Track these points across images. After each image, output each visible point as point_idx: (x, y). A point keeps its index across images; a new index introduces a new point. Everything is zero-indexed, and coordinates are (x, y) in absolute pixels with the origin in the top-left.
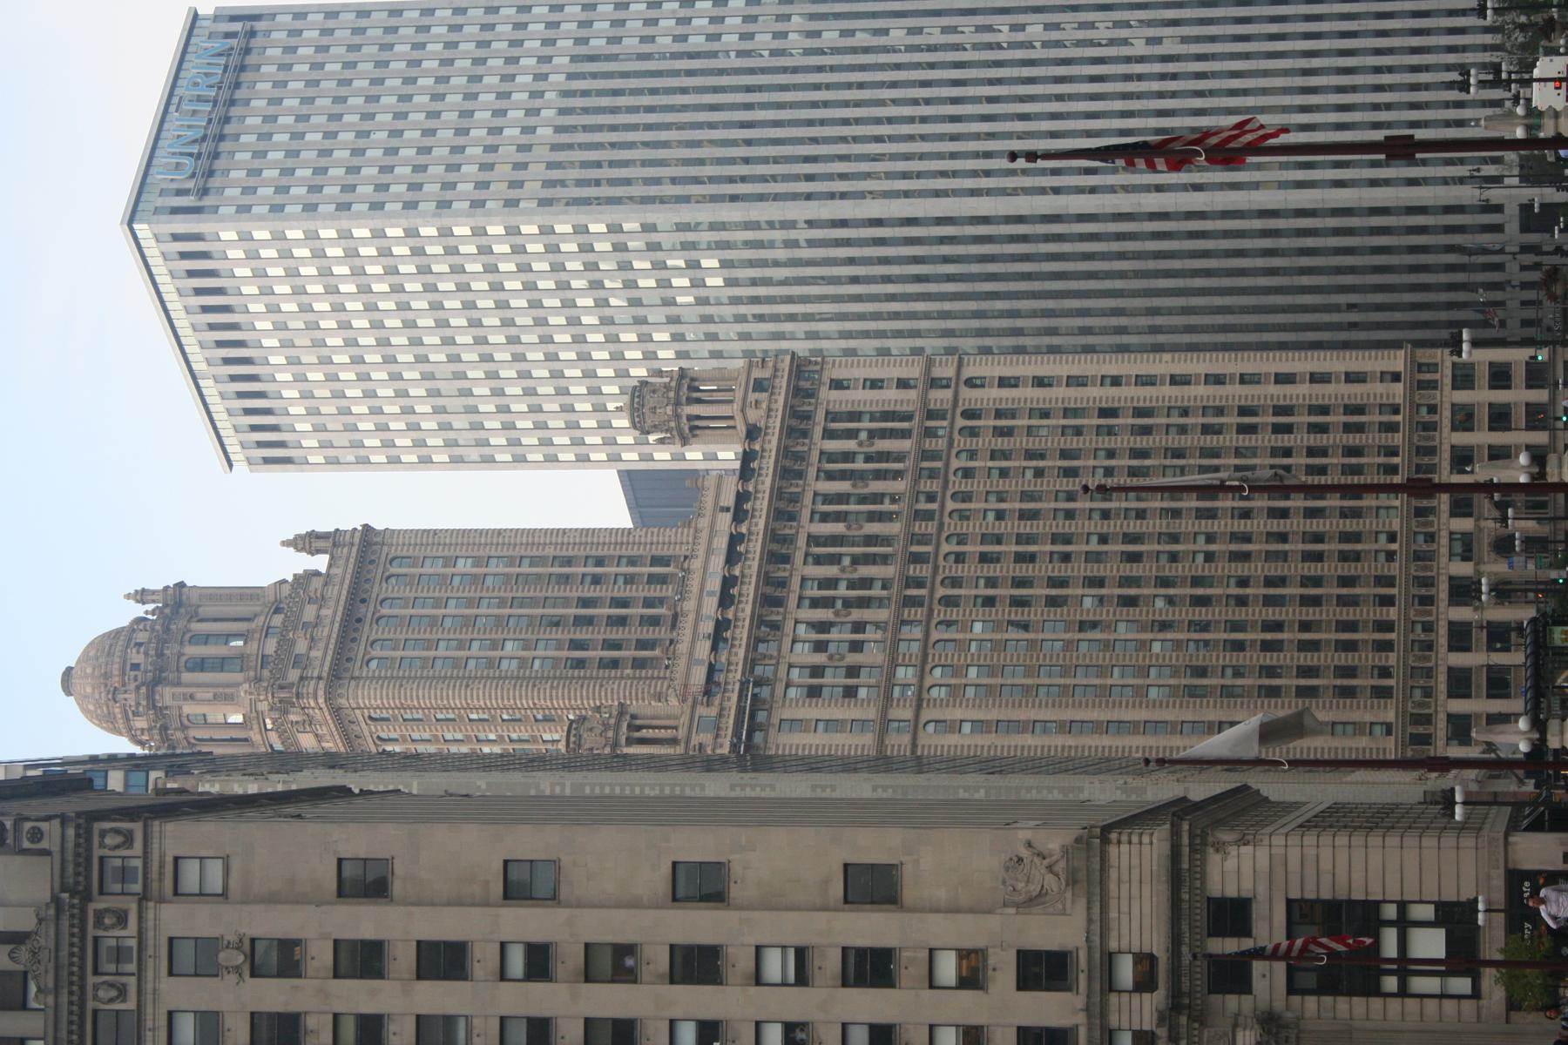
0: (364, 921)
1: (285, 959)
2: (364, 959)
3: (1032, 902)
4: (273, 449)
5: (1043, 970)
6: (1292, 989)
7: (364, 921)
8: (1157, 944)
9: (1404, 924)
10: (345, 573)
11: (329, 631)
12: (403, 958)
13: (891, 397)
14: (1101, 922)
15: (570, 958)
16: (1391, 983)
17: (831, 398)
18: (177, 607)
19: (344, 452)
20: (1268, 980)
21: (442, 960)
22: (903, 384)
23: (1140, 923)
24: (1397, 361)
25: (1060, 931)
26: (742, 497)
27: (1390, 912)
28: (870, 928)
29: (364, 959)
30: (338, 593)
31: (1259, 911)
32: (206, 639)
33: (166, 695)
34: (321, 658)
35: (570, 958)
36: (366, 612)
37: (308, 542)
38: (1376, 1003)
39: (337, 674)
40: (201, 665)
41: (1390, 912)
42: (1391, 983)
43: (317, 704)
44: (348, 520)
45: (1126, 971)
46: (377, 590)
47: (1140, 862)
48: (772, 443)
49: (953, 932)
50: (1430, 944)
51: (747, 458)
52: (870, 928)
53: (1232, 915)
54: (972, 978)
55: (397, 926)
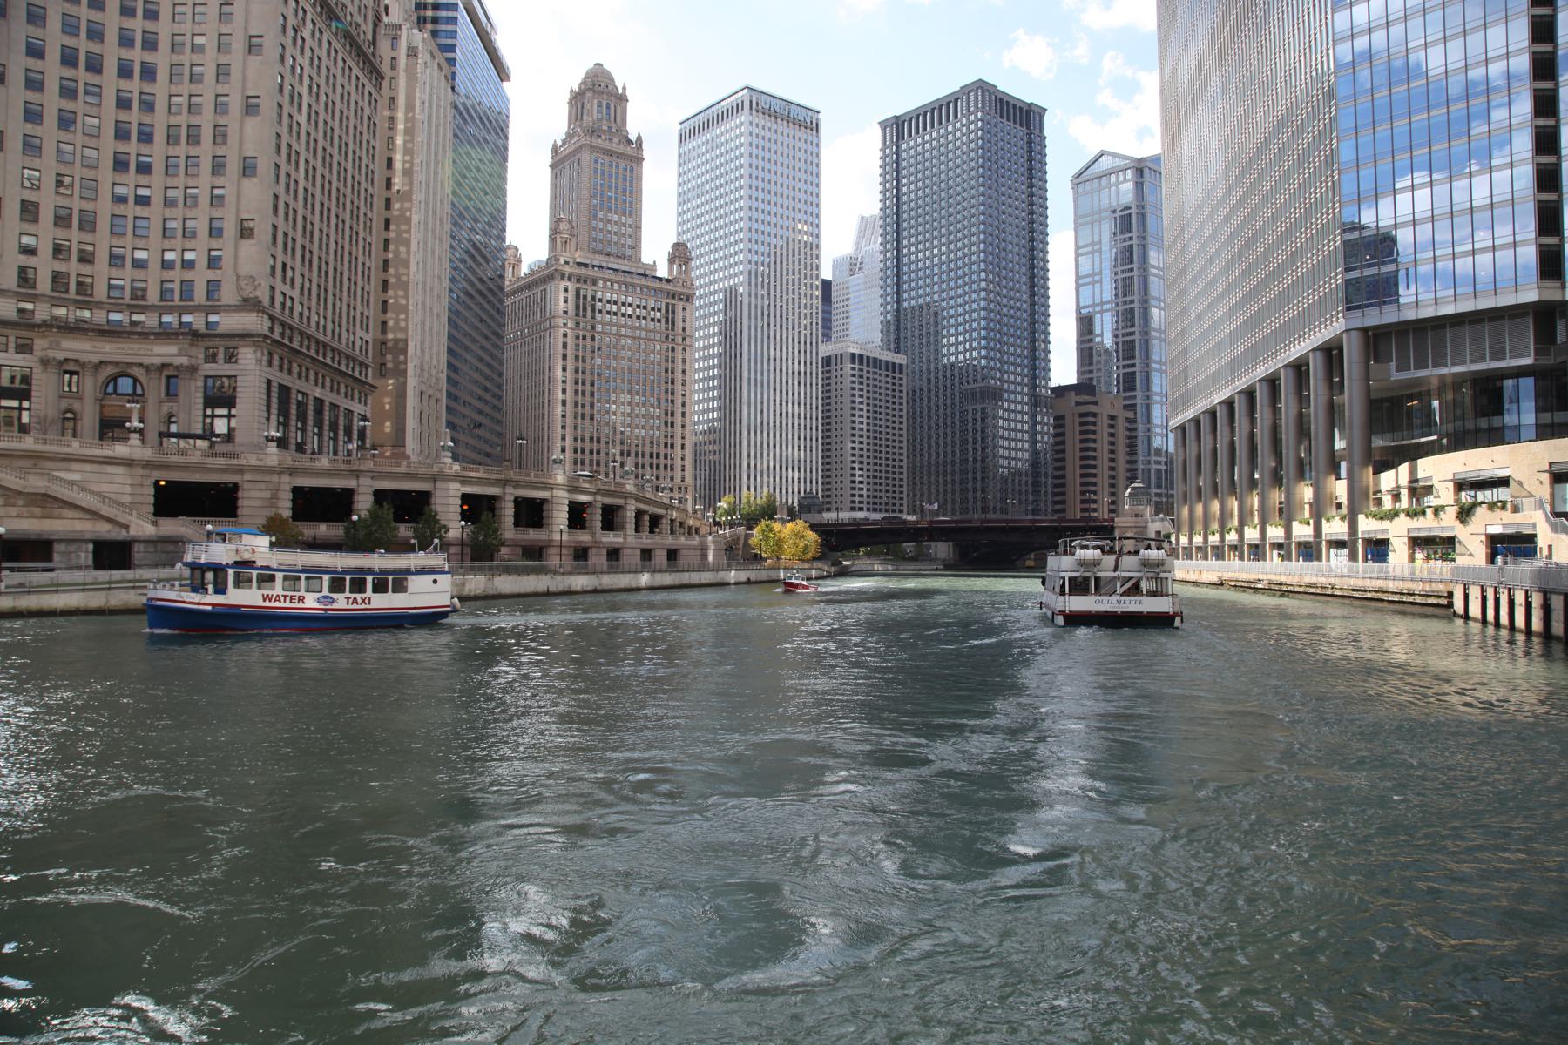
3: (239, 288)
4: (684, 137)
5: (213, 287)
6: (206, 377)
8: (221, 329)
9: (229, 416)
10: (628, 150)
11: (608, 145)
13: (679, 324)
14: (229, 309)
16: (209, 412)
17: (680, 305)
18: (622, 99)
19: (683, 160)
22: (684, 329)
23: (227, 322)
24: (689, 480)
25: (228, 295)
26: (645, 275)
27: (233, 412)
30: (621, 149)
31: (234, 366)
32: (608, 107)
33: (589, 94)
34: (599, 142)
36: (614, 158)
37: (639, 139)
38: (201, 406)
39: (593, 148)
40: (600, 105)
41: (233, 412)
42: (209, 412)
44: (647, 153)
45: (213, 318)
46: (622, 163)
47: (252, 322)
48: (664, 286)
49: (226, 255)
51: (660, 279)
53: (231, 357)
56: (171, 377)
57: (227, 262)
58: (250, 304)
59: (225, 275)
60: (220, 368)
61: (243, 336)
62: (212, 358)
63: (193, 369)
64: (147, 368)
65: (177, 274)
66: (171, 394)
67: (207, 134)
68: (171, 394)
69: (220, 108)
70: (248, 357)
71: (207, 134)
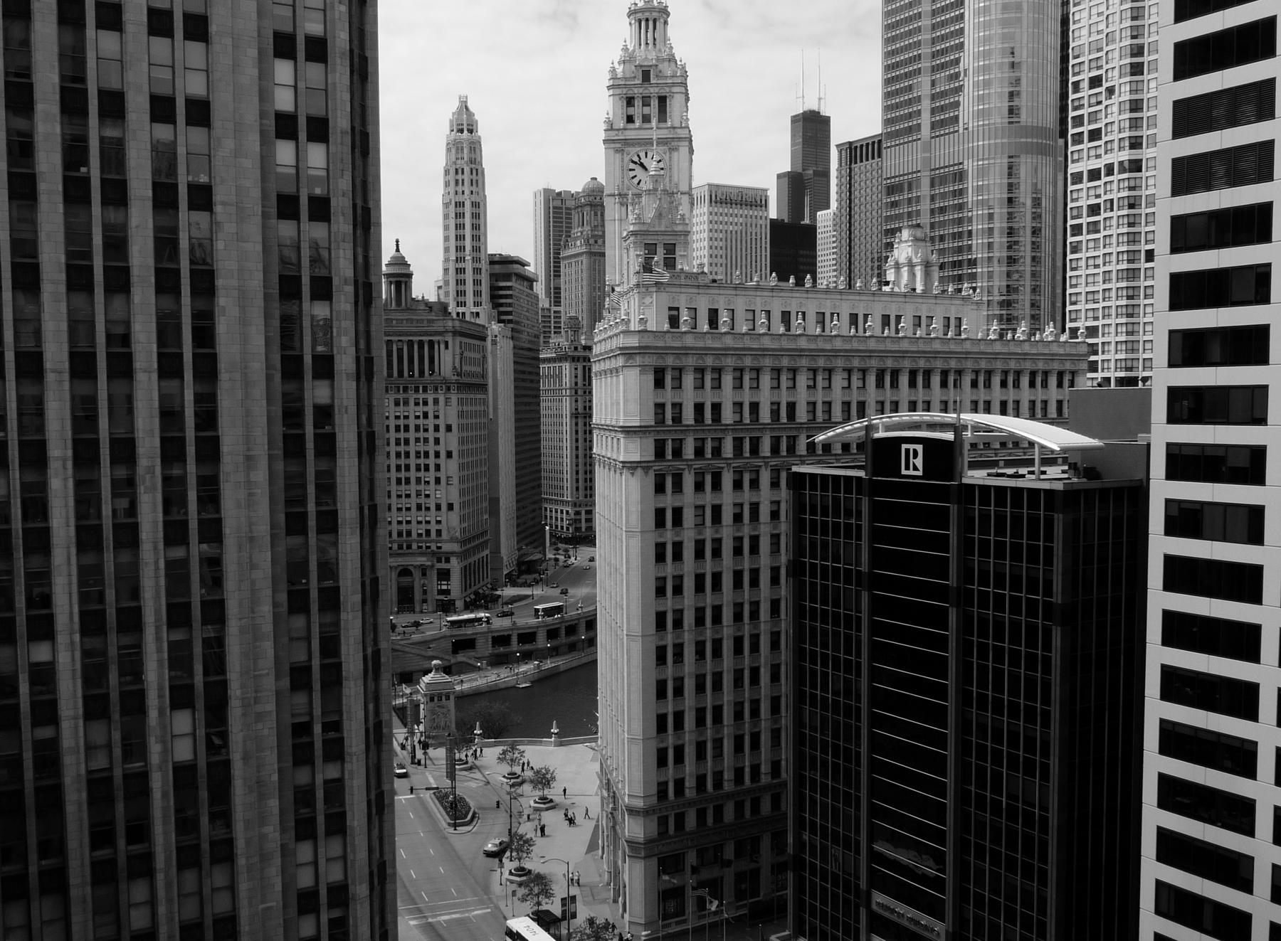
0: (442, 428)
1: (437, 417)
2: (437, 428)
5: (439, 532)
7: (442, 428)
12: (437, 435)
14: (446, 541)
15: (438, 461)
20: (439, 566)
21: (437, 441)
23: (447, 547)
25: (444, 534)
28: (444, 507)
29: (437, 428)
33: (588, 208)
35: (438, 461)
43: (584, 249)
50: (444, 587)
52: (444, 507)
53: (448, 561)
54: (439, 522)
55: (442, 434)
56: (424, 571)
57: (444, 522)
58: (452, 540)
59: (443, 527)
60: (443, 566)
61: (453, 553)
62: (439, 561)
63: (432, 566)
64: (415, 567)
65: (424, 526)
66: (424, 574)
67: (432, 468)
68: (424, 574)
69: (437, 455)
70: (454, 561)
71: (432, 468)
